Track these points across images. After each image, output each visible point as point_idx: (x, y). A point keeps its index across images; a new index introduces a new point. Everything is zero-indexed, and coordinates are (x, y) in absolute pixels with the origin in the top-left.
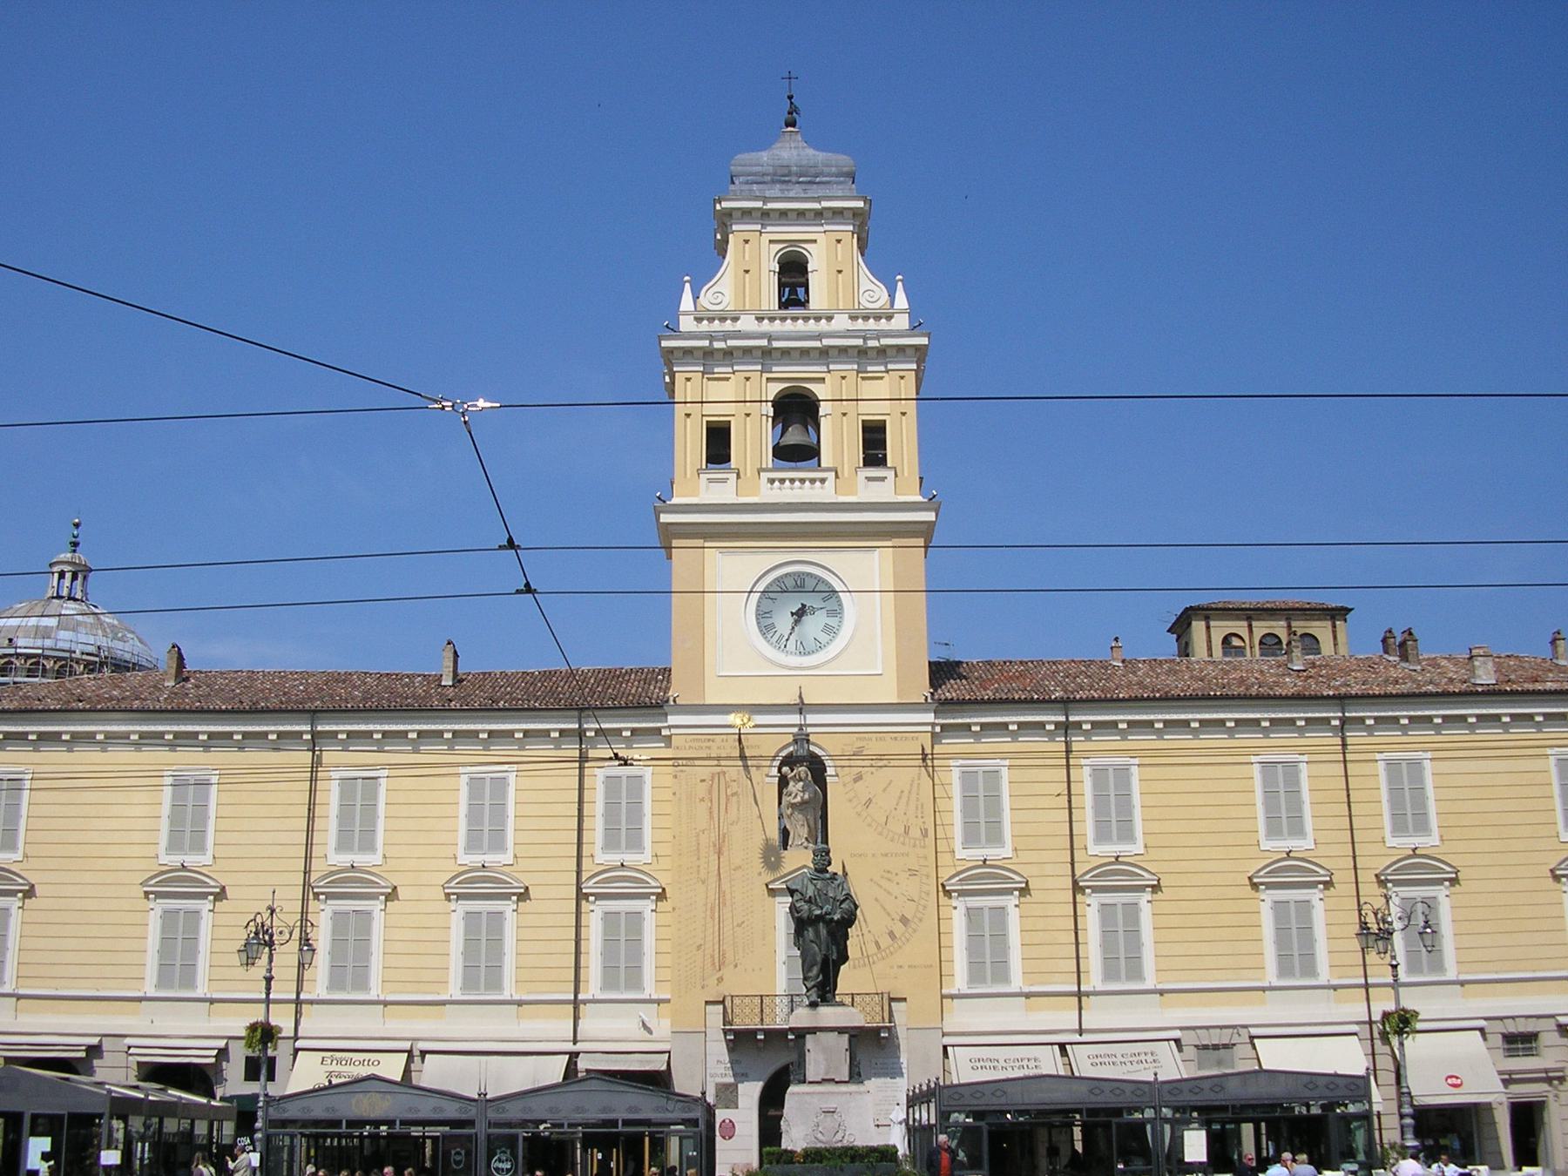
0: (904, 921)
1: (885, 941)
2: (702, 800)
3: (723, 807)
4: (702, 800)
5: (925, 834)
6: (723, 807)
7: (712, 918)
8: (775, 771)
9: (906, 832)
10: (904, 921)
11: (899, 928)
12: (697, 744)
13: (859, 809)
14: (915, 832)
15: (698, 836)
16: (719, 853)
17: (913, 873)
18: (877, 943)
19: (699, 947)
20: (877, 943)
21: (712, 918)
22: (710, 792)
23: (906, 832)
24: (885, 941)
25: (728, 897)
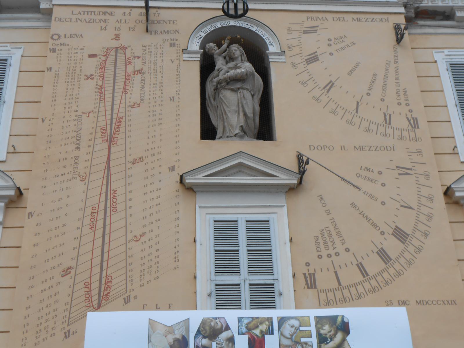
0: (400, 234)
1: (374, 265)
2: (90, 77)
3: (119, 86)
4: (90, 77)
5: (414, 124)
6: (119, 86)
7: (93, 227)
8: (196, 47)
9: (387, 120)
10: (400, 234)
11: (393, 246)
12: (87, 17)
13: (317, 93)
14: (400, 122)
15: (79, 119)
16: (111, 142)
17: (404, 171)
18: (361, 267)
19: (67, 272)
20: (361, 267)
21: (93, 227)
22: (102, 67)
23: (387, 120)
24: (374, 265)
25: (120, 199)
